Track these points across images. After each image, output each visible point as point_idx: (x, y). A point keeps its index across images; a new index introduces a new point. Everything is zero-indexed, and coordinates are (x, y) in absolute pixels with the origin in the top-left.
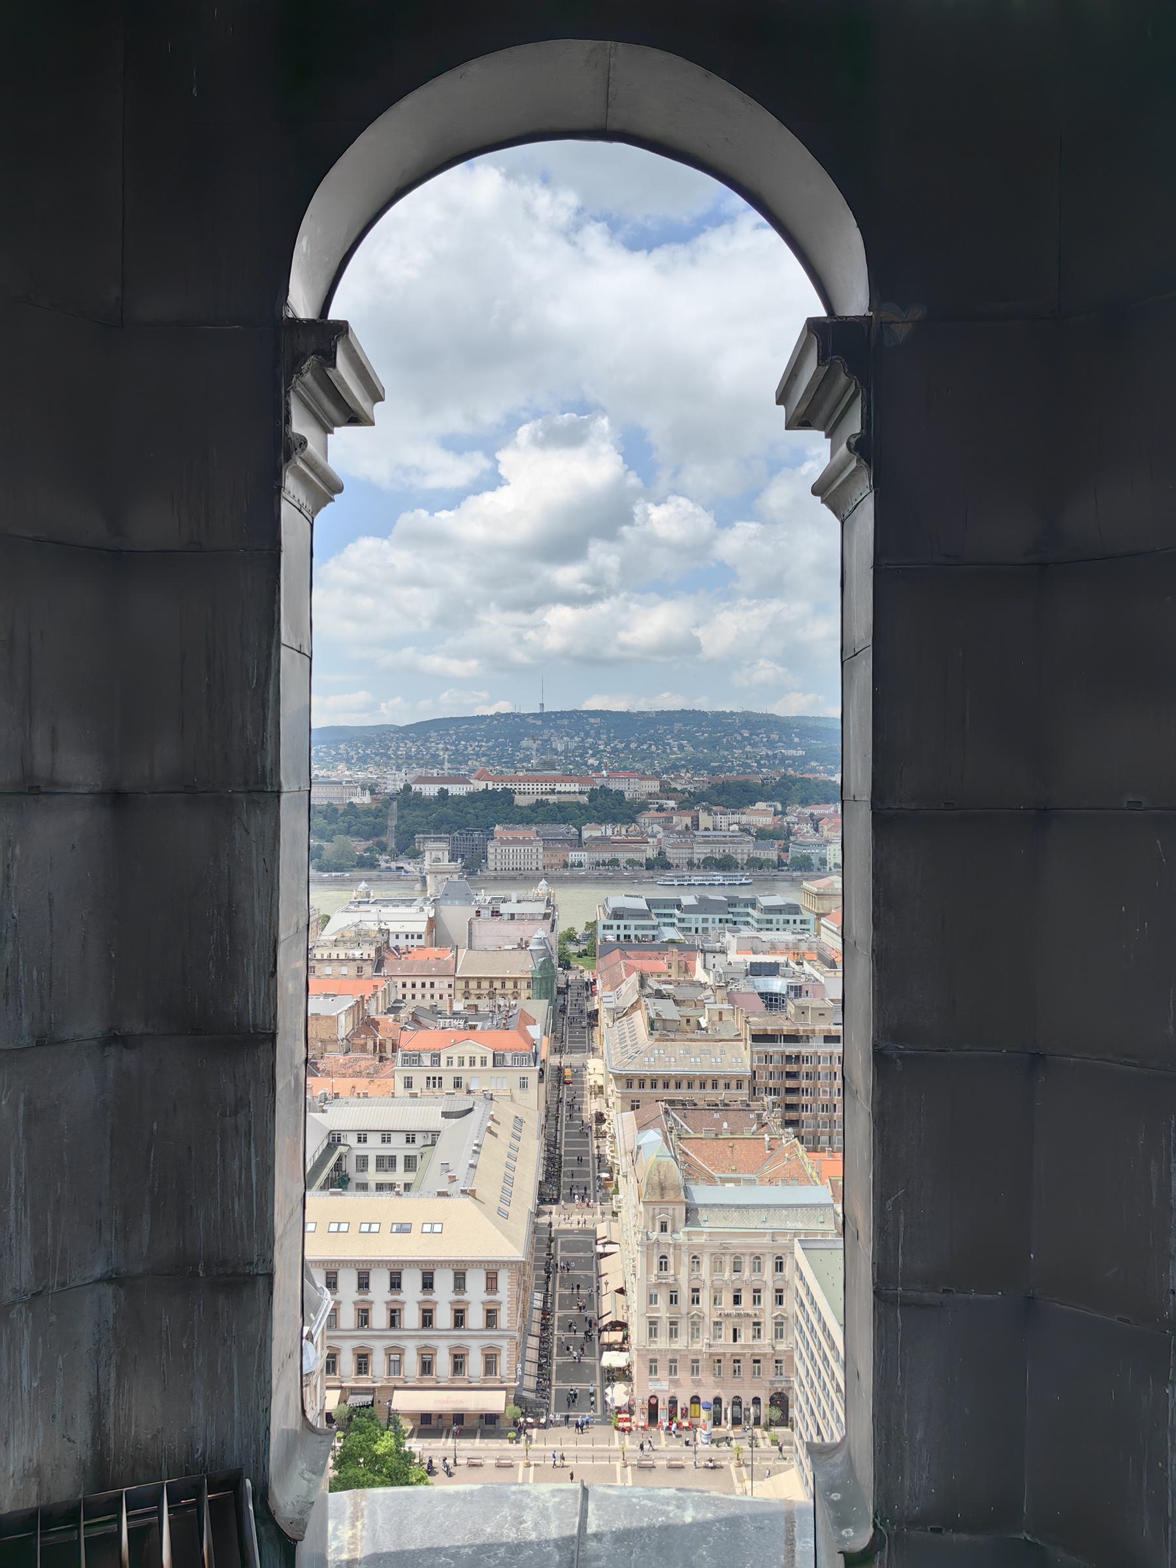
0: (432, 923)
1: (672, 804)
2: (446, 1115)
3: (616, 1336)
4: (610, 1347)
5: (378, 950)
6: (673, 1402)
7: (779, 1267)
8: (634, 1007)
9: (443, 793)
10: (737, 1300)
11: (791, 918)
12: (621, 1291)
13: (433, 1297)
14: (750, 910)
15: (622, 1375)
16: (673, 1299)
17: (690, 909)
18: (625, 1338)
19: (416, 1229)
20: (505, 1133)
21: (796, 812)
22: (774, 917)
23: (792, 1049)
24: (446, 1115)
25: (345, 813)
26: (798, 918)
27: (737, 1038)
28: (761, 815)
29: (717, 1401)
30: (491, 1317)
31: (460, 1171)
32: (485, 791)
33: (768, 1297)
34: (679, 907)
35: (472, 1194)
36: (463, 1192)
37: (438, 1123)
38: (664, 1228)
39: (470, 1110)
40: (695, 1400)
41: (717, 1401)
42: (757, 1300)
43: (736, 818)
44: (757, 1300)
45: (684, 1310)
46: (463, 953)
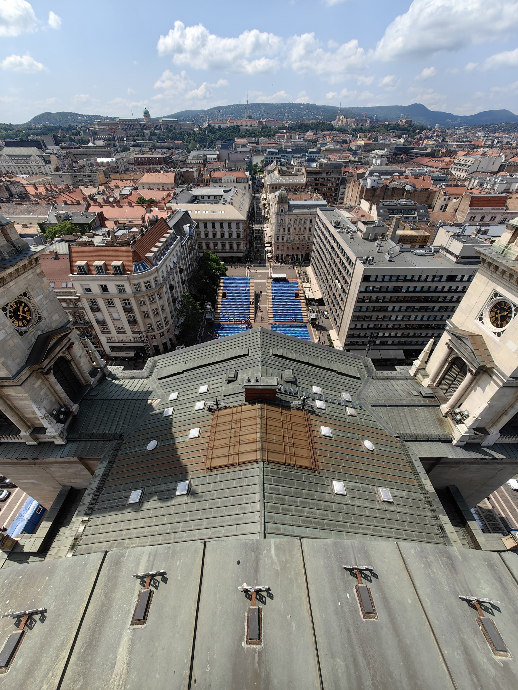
0: (218, 155)
1: (285, 131)
2: (224, 191)
3: (269, 245)
4: (267, 247)
5: (204, 161)
6: (282, 255)
7: (311, 222)
8: (275, 169)
9: (220, 127)
10: (300, 231)
12: (270, 236)
13: (224, 230)
14: (307, 154)
15: (270, 252)
16: (284, 231)
17: (290, 153)
18: (271, 245)
19: (218, 212)
20: (240, 195)
21: (320, 134)
23: (317, 177)
24: (224, 191)
25: (193, 134)
26: (319, 155)
27: (303, 174)
28: (309, 135)
29: (293, 255)
30: (238, 235)
31: (229, 201)
32: (231, 126)
33: (307, 229)
34: (287, 153)
35: (232, 204)
36: (229, 203)
37: (222, 193)
38: (282, 211)
39: (231, 190)
40: (287, 255)
41: (293, 255)
42: (304, 231)
43: (303, 136)
44: (304, 231)
45: (286, 233)
46: (227, 162)
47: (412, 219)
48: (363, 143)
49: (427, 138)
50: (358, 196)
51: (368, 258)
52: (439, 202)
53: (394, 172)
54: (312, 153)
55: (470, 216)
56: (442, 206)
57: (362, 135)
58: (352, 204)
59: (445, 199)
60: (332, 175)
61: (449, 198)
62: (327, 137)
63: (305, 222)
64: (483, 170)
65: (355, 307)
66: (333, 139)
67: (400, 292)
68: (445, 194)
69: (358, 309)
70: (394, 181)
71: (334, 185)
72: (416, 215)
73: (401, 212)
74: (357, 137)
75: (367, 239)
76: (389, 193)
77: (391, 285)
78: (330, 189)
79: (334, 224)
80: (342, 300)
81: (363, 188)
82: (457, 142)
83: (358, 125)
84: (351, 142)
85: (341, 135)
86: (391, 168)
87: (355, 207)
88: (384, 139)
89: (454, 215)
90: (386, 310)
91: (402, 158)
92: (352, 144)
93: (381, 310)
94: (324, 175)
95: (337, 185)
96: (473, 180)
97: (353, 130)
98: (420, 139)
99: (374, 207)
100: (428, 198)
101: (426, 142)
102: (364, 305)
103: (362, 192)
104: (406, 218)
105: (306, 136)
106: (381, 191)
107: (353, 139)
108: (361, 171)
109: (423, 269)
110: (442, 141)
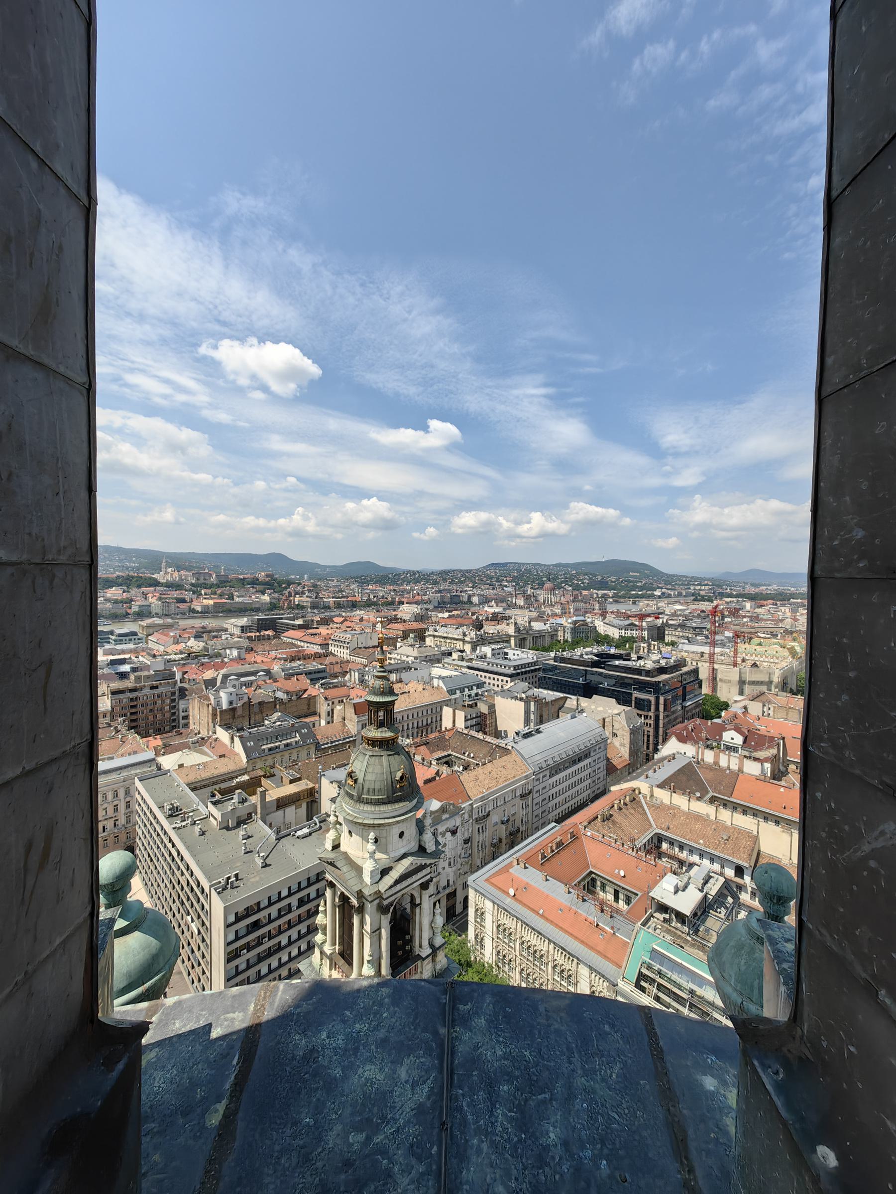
7: (127, 792)
11: (133, 638)
14: (111, 636)
21: (134, 591)
22: (124, 638)
23: (133, 695)
47: (294, 744)
48: (211, 602)
49: (298, 594)
50: (210, 721)
51: (229, 878)
52: (323, 708)
53: (258, 672)
54: (120, 635)
55: (360, 724)
56: (329, 712)
57: (209, 591)
58: (204, 733)
59: (328, 705)
60: (161, 689)
61: (333, 703)
62: (150, 595)
63: (116, 795)
64: (364, 645)
65: (226, 971)
66: (160, 599)
67: (290, 911)
68: (326, 699)
69: (234, 972)
70: (260, 688)
71: (168, 701)
72: (298, 738)
73: (277, 739)
74: (201, 594)
75: (228, 828)
76: (256, 709)
77: (274, 911)
78: (162, 709)
79: (169, 813)
80: (204, 957)
81: (214, 710)
82: (333, 598)
83: (198, 579)
84: (191, 601)
85: (174, 592)
86: (253, 667)
87: (209, 737)
88: (243, 596)
89: (344, 725)
90: (279, 948)
91: (268, 635)
92: (195, 603)
93: (270, 953)
94: (147, 691)
95: (174, 701)
96: (353, 673)
97: (192, 585)
98: (290, 595)
99: (237, 740)
100: (309, 705)
101: (297, 599)
102: (241, 962)
103: (214, 715)
104: (287, 745)
105: (109, 595)
106: (243, 709)
107: (195, 596)
108: (209, 674)
109: (308, 869)
110: (316, 598)
